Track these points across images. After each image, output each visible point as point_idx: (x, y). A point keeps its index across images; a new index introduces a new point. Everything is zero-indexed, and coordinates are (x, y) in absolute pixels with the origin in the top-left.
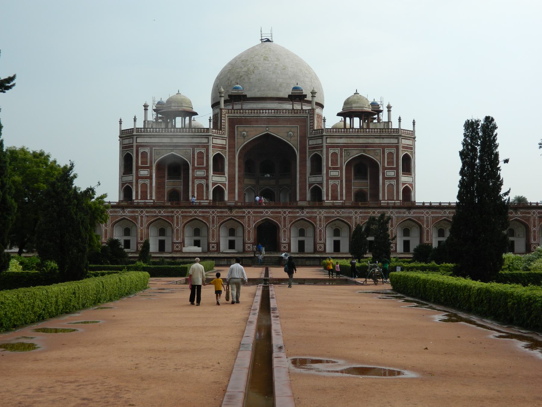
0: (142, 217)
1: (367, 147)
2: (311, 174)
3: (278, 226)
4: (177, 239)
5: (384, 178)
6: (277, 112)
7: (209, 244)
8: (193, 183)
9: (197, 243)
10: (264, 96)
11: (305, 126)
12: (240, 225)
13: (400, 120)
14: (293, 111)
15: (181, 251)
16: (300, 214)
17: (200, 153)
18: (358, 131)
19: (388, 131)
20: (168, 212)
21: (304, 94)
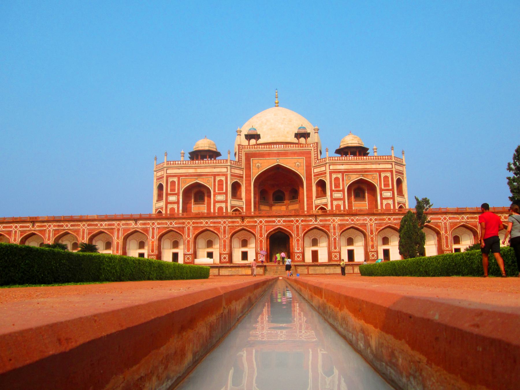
0: (153, 229)
1: (365, 172)
2: (316, 198)
3: (291, 235)
4: (188, 251)
5: (382, 199)
7: (220, 254)
9: (210, 255)
10: (275, 141)
11: (310, 157)
12: (253, 236)
13: (392, 147)
15: (193, 262)
16: (313, 223)
17: (221, 181)
20: (180, 223)
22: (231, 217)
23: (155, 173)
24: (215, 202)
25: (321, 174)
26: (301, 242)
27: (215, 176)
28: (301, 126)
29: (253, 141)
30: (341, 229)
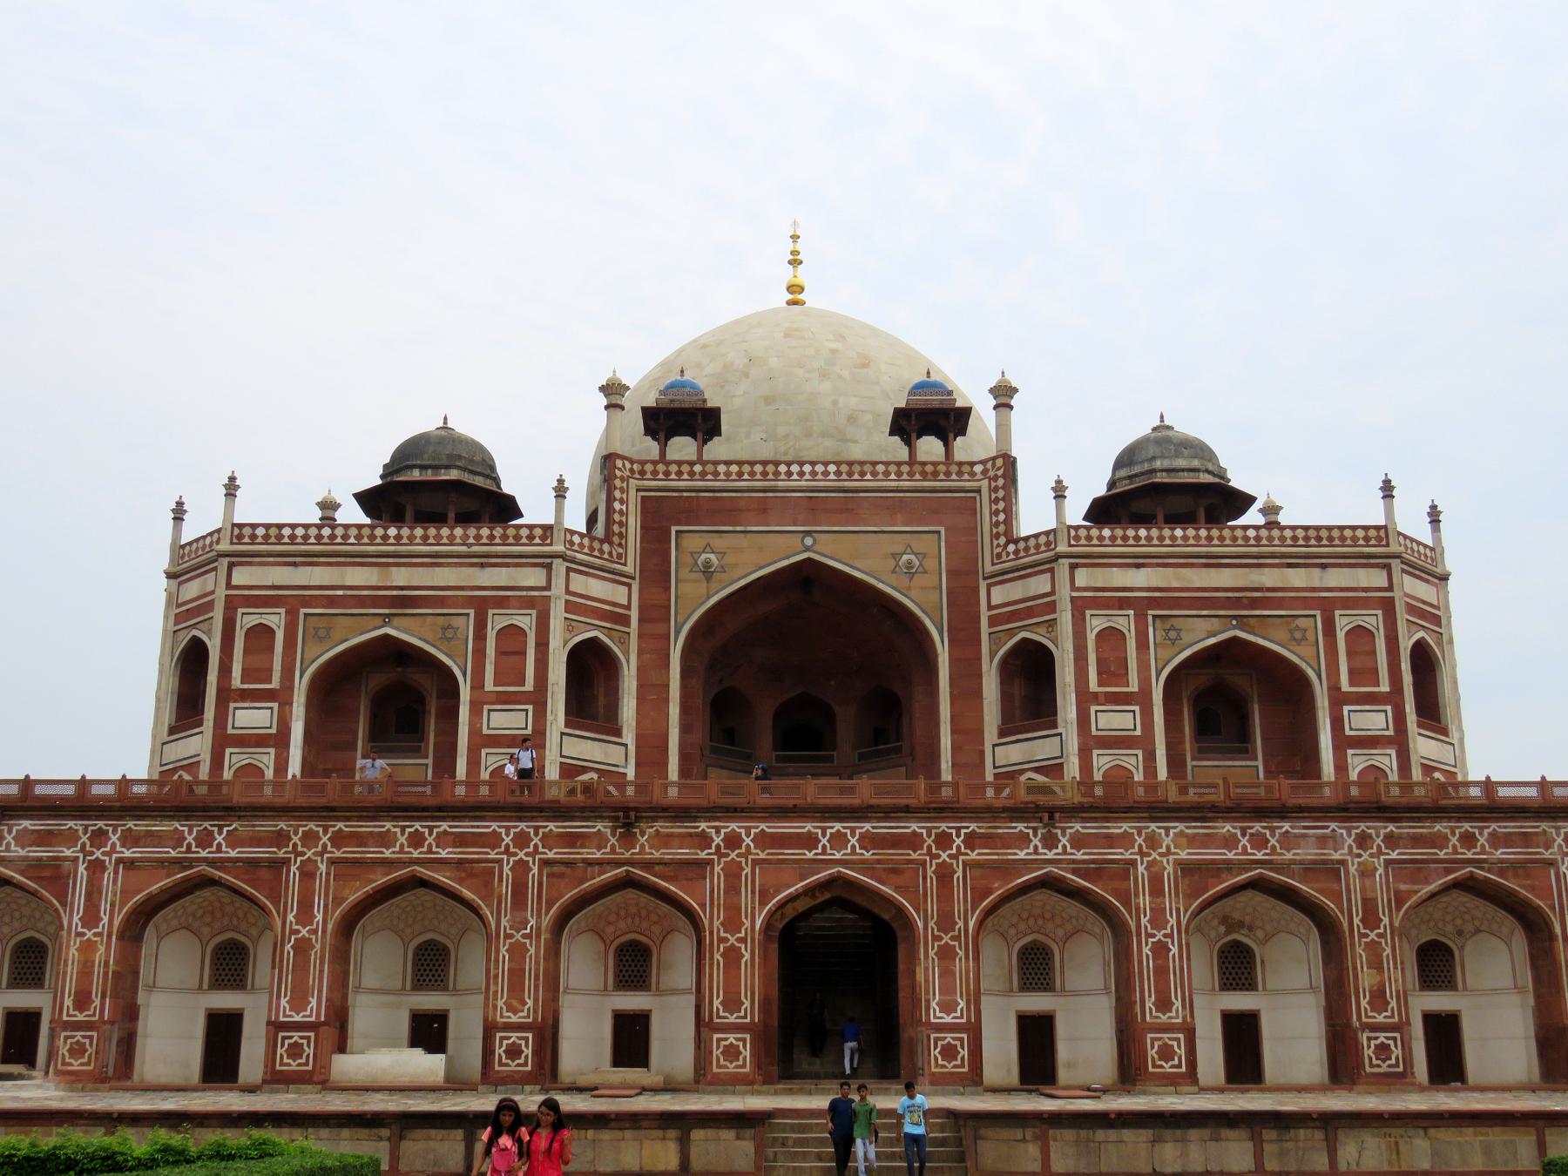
0: (96, 867)
1: (1254, 603)
3: (908, 924)
4: (298, 1003)
5: (1343, 743)
6: (850, 474)
7: (490, 1029)
8: (474, 763)
9: (428, 1032)
11: (972, 530)
12: (682, 921)
13: (1387, 489)
14: (917, 468)
16: (1034, 851)
18: (1209, 538)
19: (1343, 538)
20: (257, 841)
21: (958, 404)
22: (558, 812)
23: (174, 583)
24: (480, 740)
25: (1030, 613)
26: (958, 966)
27: (483, 605)
28: (922, 378)
29: (682, 447)
30: (1193, 894)
